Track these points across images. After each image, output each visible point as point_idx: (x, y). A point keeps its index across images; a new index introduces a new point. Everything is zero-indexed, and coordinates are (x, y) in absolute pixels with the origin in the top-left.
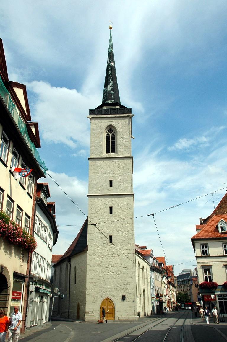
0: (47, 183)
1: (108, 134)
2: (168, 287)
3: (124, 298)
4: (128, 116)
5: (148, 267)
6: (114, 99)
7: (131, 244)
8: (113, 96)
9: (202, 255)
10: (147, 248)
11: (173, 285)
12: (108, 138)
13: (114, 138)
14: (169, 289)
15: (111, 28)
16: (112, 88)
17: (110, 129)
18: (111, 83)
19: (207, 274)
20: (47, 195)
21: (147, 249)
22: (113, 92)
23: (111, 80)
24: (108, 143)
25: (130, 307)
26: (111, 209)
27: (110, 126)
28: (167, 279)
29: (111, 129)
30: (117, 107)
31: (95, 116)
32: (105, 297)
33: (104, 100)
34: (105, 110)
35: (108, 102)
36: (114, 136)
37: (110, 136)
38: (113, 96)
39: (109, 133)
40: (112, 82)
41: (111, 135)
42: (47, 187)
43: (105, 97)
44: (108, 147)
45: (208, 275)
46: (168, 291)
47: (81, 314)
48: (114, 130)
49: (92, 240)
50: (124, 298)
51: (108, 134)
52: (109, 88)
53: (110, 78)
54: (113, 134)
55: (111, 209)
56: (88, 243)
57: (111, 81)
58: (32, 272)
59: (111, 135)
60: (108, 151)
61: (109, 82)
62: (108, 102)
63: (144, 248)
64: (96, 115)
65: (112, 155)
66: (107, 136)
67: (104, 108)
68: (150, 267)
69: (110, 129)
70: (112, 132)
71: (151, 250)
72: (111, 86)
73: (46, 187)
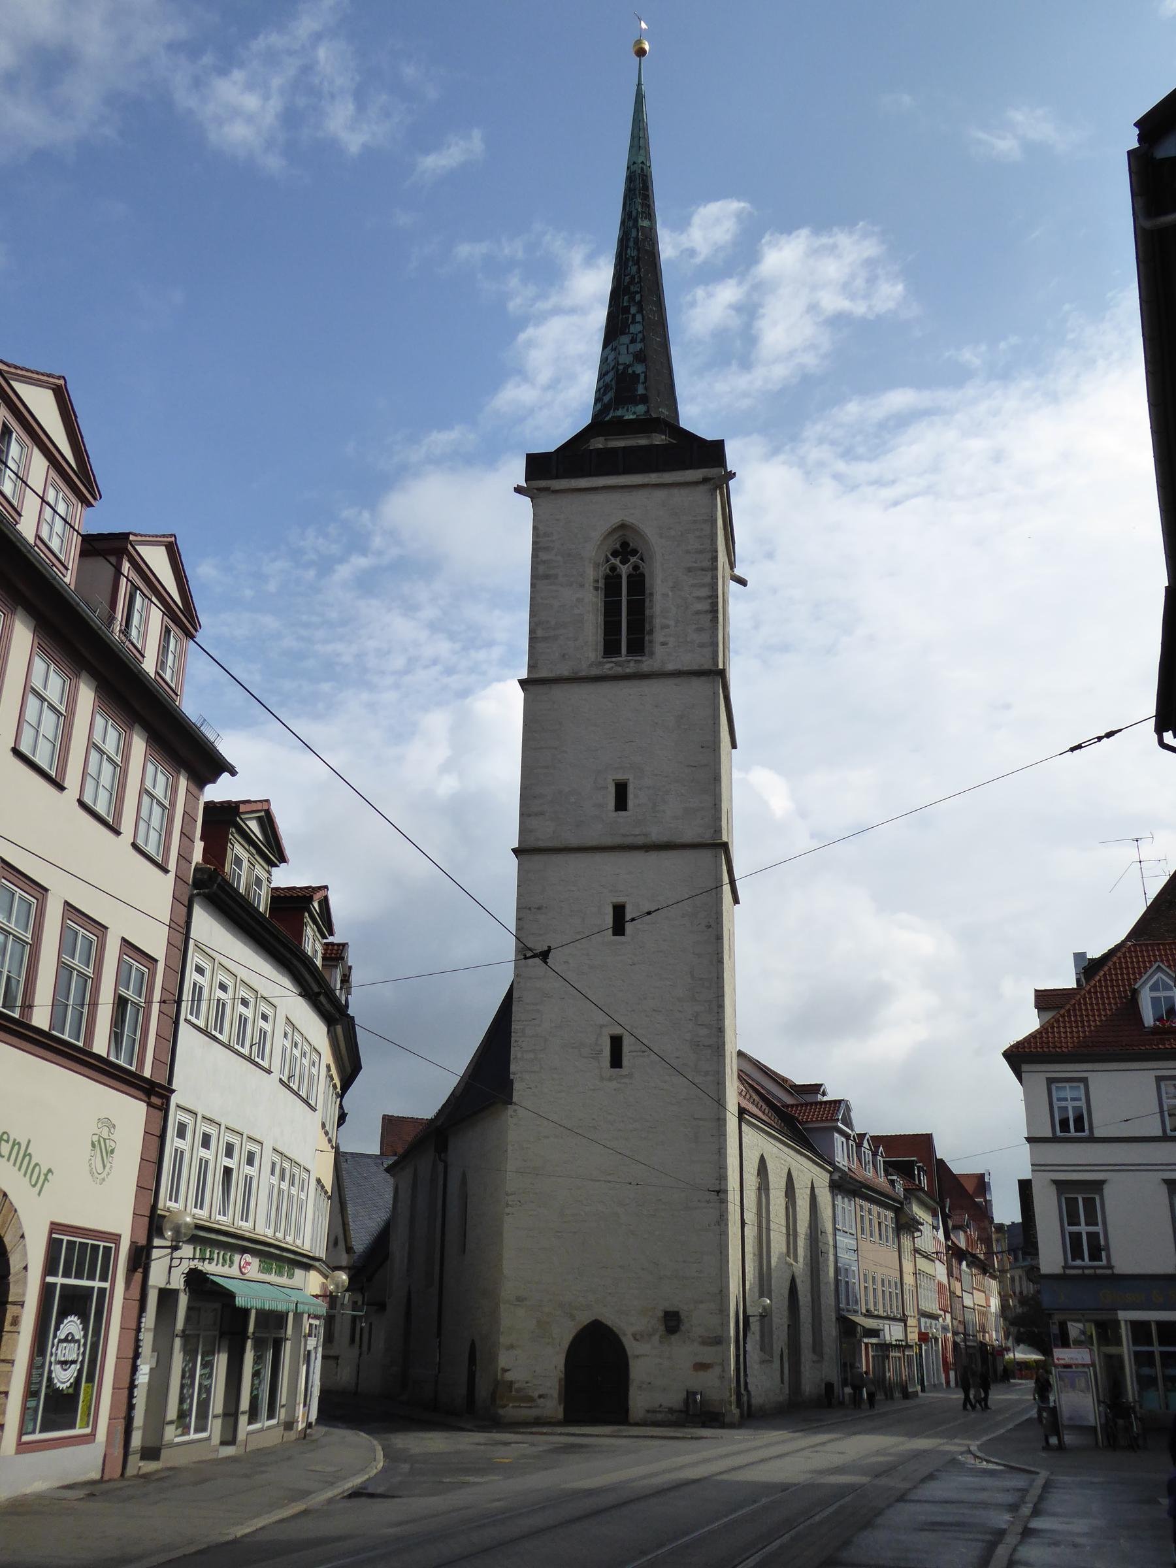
0: (267, 801)
1: (613, 568)
2: (950, 1274)
3: (672, 1322)
4: (705, 480)
5: (822, 1179)
7: (707, 1073)
9: (1058, 1133)
10: (828, 1091)
11: (984, 1268)
12: (611, 585)
13: (638, 583)
14: (958, 1285)
17: (625, 544)
18: (633, 322)
19: (1079, 1225)
20: (272, 850)
21: (825, 1099)
22: (639, 369)
23: (633, 310)
25: (701, 1367)
27: (623, 526)
28: (947, 1237)
29: (625, 544)
30: (659, 439)
32: (585, 1319)
33: (599, 406)
34: (599, 451)
35: (619, 413)
36: (642, 575)
37: (620, 576)
39: (616, 561)
41: (624, 570)
42: (267, 822)
43: (605, 394)
45: (1083, 1229)
46: (952, 1293)
47: (483, 1391)
49: (531, 1056)
50: (672, 1322)
51: (613, 568)
52: (623, 349)
54: (636, 568)
56: (513, 1068)
57: (634, 316)
58: (164, 1202)
59: (624, 570)
60: (611, 648)
61: (627, 319)
62: (619, 413)
63: (816, 1088)
64: (557, 477)
65: (625, 662)
66: (607, 577)
67: (598, 443)
68: (831, 1181)
69: (625, 544)
70: (633, 560)
71: (840, 1101)
72: (633, 341)
73: (259, 819)
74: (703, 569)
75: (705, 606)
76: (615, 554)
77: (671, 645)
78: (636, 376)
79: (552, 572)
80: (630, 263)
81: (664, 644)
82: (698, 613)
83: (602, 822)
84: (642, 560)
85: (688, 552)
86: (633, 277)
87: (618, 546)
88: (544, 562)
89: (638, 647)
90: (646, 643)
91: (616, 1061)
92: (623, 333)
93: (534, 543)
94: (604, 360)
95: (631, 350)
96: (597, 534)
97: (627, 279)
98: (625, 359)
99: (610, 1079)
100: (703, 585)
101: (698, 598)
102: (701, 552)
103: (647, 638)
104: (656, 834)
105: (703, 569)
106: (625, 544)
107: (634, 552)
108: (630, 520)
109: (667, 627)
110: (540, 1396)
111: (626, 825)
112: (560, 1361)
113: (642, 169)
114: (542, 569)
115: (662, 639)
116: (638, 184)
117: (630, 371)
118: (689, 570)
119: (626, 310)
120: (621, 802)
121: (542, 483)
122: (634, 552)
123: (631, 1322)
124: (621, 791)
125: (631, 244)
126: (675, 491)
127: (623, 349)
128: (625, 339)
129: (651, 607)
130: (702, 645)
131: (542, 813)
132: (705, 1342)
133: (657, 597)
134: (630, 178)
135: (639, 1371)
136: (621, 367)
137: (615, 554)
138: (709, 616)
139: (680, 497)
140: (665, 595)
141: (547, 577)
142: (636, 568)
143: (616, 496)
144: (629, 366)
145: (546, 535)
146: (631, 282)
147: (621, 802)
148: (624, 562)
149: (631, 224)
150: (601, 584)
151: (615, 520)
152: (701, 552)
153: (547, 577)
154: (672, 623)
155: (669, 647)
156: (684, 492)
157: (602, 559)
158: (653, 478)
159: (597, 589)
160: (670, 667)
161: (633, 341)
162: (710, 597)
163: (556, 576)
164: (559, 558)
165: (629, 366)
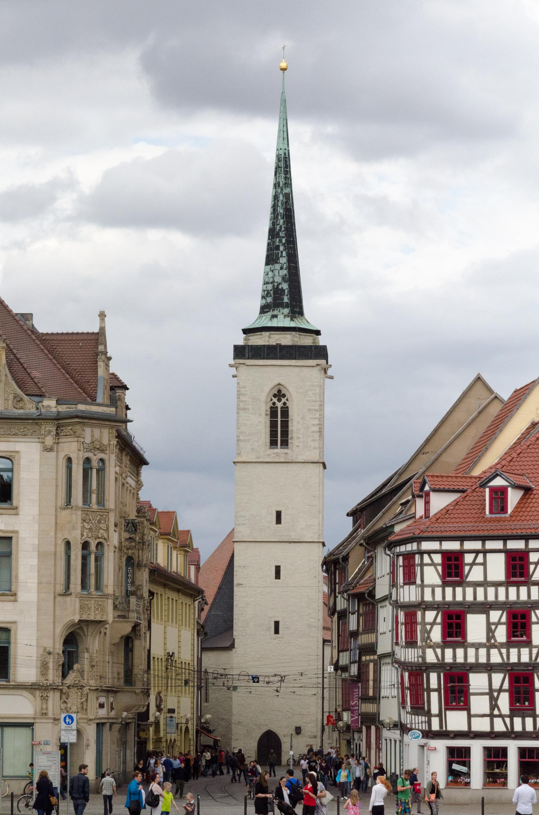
6: (287, 305)
8: (286, 299)
12: (273, 412)
13: (285, 412)
17: (279, 391)
23: (282, 248)
24: (273, 425)
36: (287, 407)
37: (277, 407)
38: (286, 299)
40: (284, 254)
41: (279, 405)
48: (288, 395)
50: (298, 730)
51: (274, 404)
52: (276, 272)
53: (280, 241)
54: (285, 404)
57: (282, 252)
59: (279, 405)
60: (273, 443)
61: (278, 253)
66: (271, 407)
69: (279, 391)
70: (284, 400)
72: (282, 268)
74: (315, 410)
75: (316, 429)
76: (275, 396)
77: (301, 447)
78: (283, 290)
79: (247, 407)
80: (279, 217)
81: (298, 446)
82: (313, 432)
84: (287, 400)
85: (309, 401)
86: (281, 226)
87: (276, 392)
88: (243, 401)
89: (285, 443)
90: (289, 444)
92: (277, 263)
93: (238, 391)
95: (281, 274)
96: (267, 389)
97: (278, 228)
98: (278, 279)
99: (275, 639)
100: (316, 418)
101: (314, 425)
102: (315, 401)
103: (290, 441)
104: (294, 537)
105: (315, 410)
107: (284, 396)
108: (282, 383)
109: (299, 438)
110: (248, 757)
112: (255, 744)
113: (285, 154)
114: (242, 405)
115: (297, 444)
116: (282, 164)
117: (280, 287)
118: (309, 410)
119: (278, 248)
120: (279, 520)
121: (242, 361)
122: (284, 396)
123: (284, 733)
125: (280, 204)
126: (304, 369)
127: (276, 272)
128: (278, 266)
129: (292, 426)
130: (315, 448)
131: (245, 524)
132: (310, 737)
133: (295, 423)
135: (285, 746)
136: (276, 284)
137: (275, 396)
138: (318, 434)
140: (298, 422)
141: (244, 409)
142: (285, 404)
143: (276, 369)
144: (280, 284)
145: (244, 387)
146: (280, 230)
147: (279, 520)
148: (279, 400)
149: (279, 190)
150: (269, 413)
151: (276, 382)
152: (315, 401)
153: (244, 409)
154: (301, 436)
156: (307, 369)
157: (269, 399)
159: (267, 415)
160: (301, 458)
161: (282, 268)
162: (319, 425)
163: (248, 409)
164: (250, 400)
165: (280, 284)
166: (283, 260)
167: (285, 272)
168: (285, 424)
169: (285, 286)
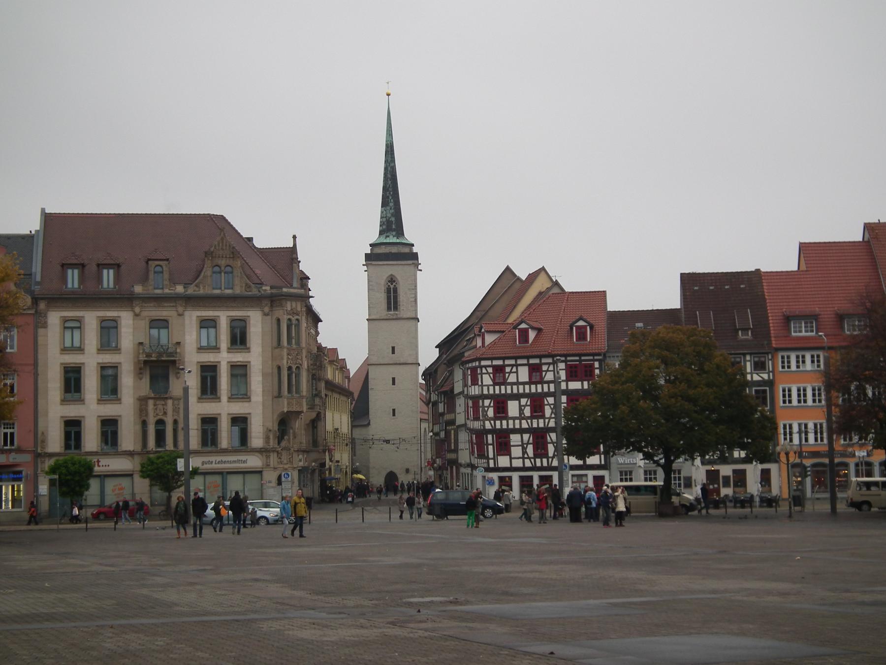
3: (407, 471)
6: (394, 230)
12: (388, 291)
15: (388, 95)
16: (392, 211)
24: (389, 298)
26: (394, 379)
29: (392, 280)
31: (374, 263)
32: (388, 471)
41: (392, 287)
44: (389, 303)
50: (407, 471)
55: (394, 379)
59: (392, 287)
60: (389, 309)
83: (388, 357)
89: (396, 308)
91: (394, 415)
94: (382, 212)
96: (385, 278)
104: (402, 361)
106: (392, 280)
111: (396, 358)
119: (388, 197)
120: (393, 352)
124: (393, 348)
134: (387, 145)
139: (406, 268)
147: (393, 352)
155: (404, 311)
158: (399, 262)
160: (405, 316)
166: (391, 204)
167: (392, 211)
168: (396, 298)
169: (393, 219)
